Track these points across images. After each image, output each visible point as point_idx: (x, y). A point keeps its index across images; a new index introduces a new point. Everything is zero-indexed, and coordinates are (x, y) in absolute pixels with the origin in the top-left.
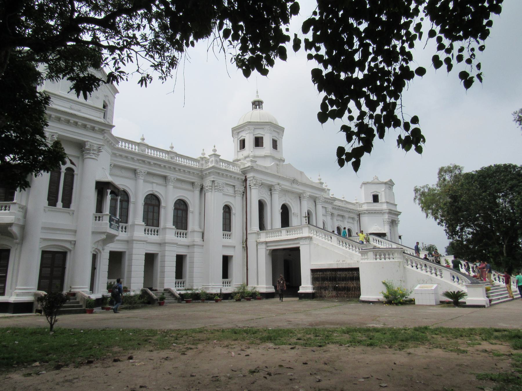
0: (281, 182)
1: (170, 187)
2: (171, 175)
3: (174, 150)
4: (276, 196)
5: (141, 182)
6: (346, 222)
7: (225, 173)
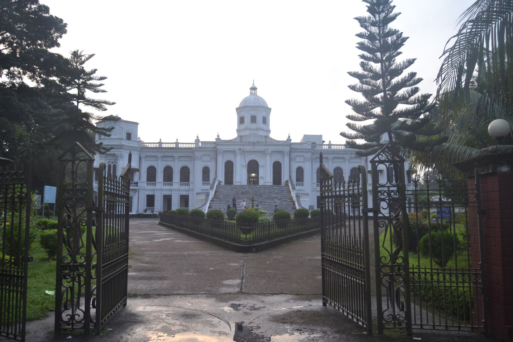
0: (242, 147)
1: (176, 161)
2: (176, 155)
3: (178, 141)
4: (238, 157)
5: (160, 161)
6: (347, 163)
7: (201, 149)
